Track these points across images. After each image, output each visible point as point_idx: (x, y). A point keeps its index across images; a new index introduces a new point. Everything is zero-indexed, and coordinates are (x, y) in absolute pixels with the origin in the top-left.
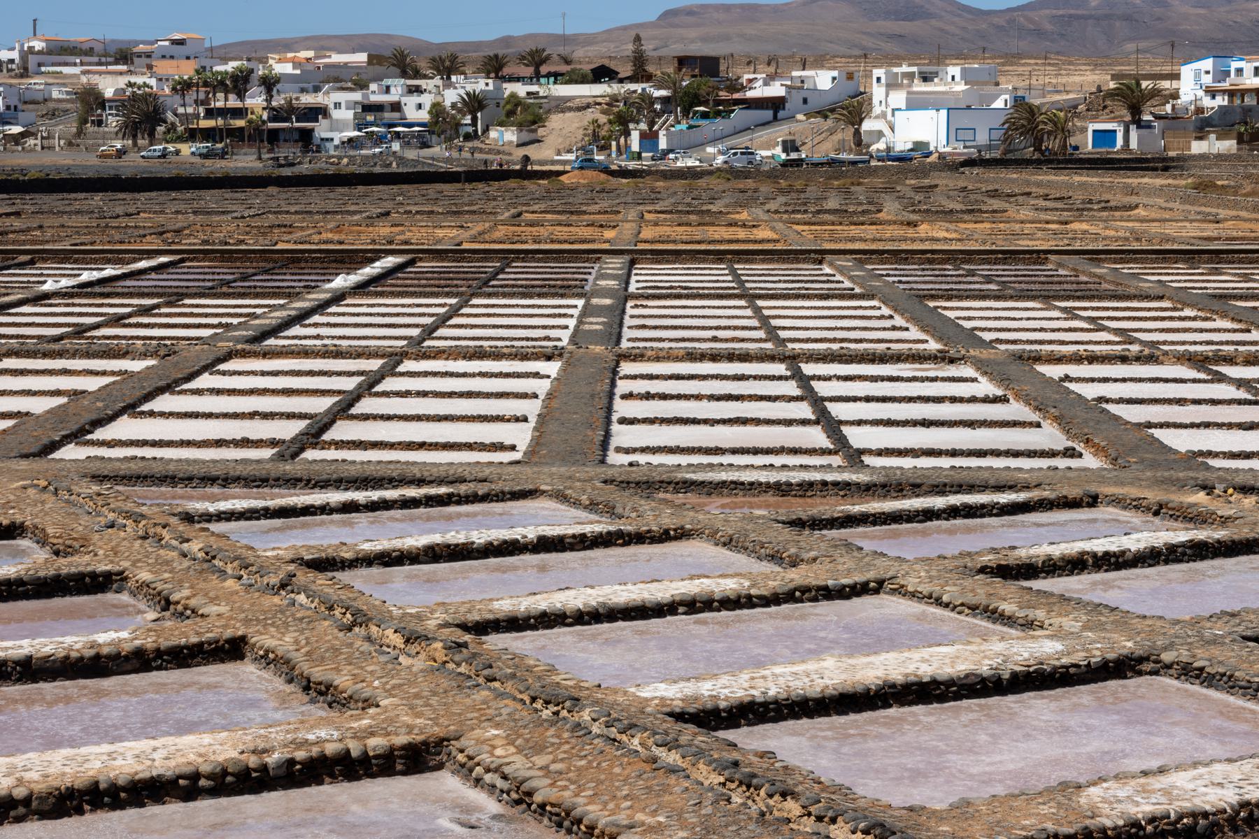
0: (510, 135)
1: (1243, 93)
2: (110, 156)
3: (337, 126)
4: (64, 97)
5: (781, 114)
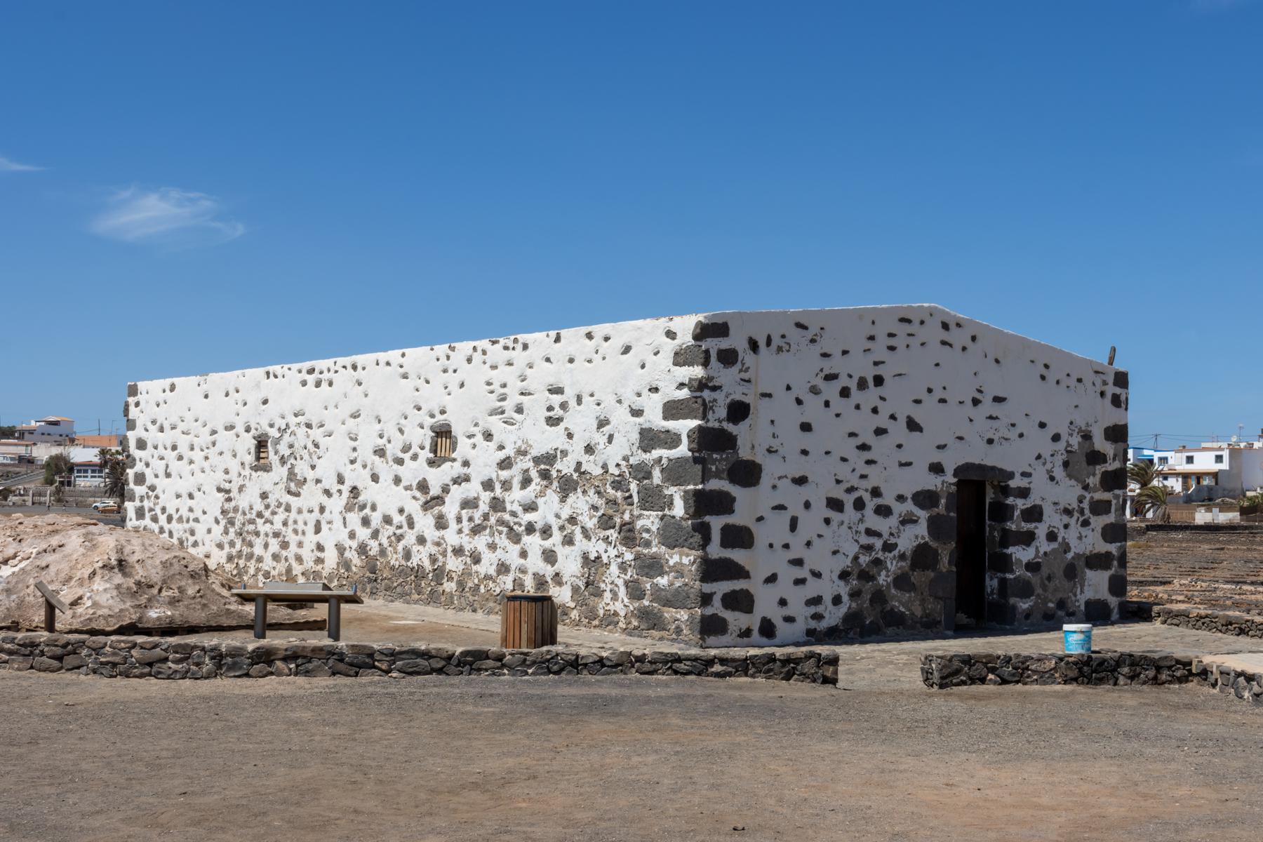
1: (1199, 476)
2: (112, 511)
4: (9, 462)
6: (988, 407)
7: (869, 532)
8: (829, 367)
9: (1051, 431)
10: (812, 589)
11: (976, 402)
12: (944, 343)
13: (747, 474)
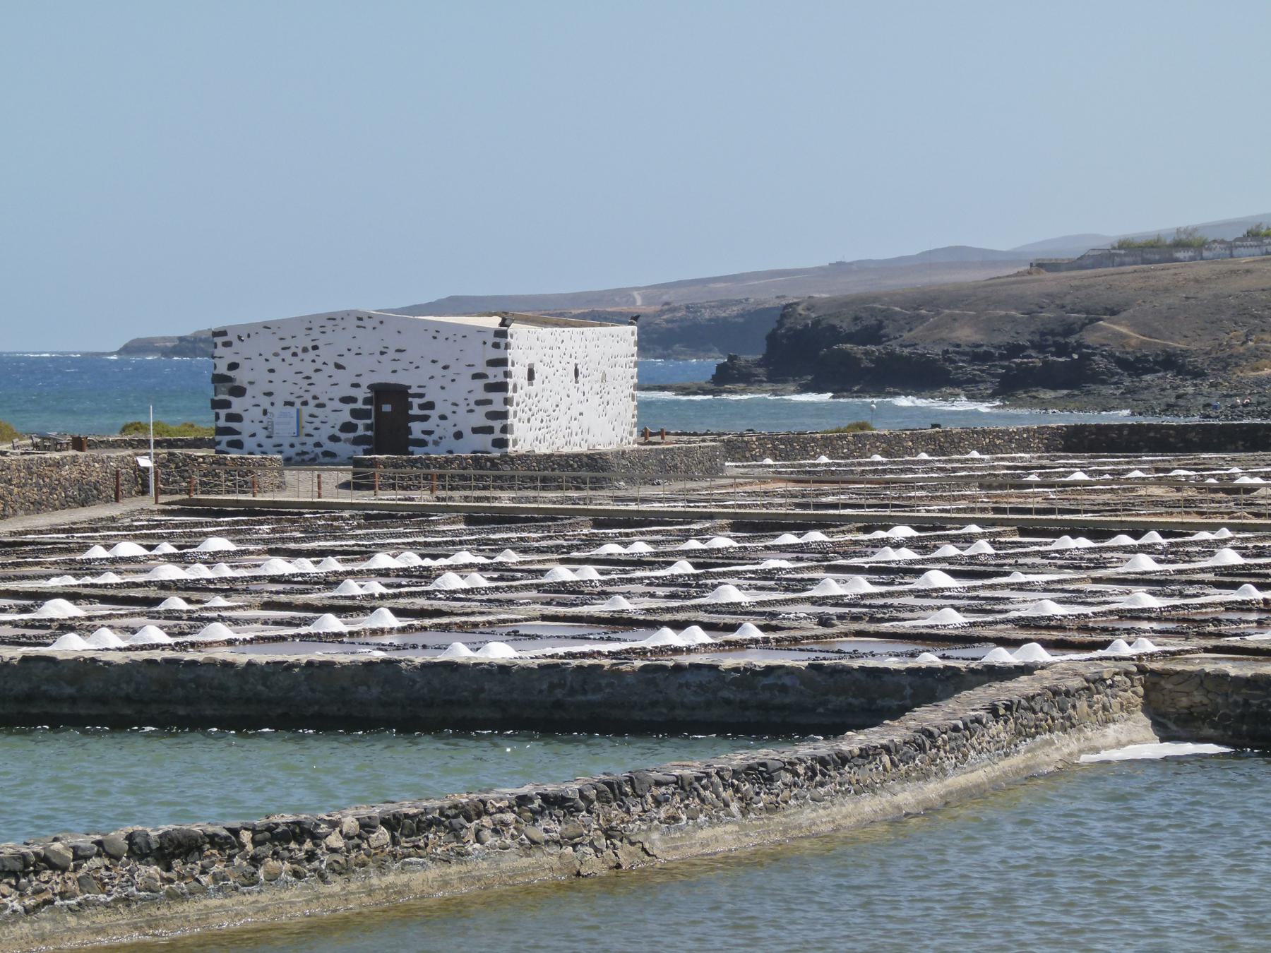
6: (391, 354)
7: (312, 416)
8: (284, 344)
9: (441, 364)
11: (382, 353)
12: (358, 327)
13: (239, 392)
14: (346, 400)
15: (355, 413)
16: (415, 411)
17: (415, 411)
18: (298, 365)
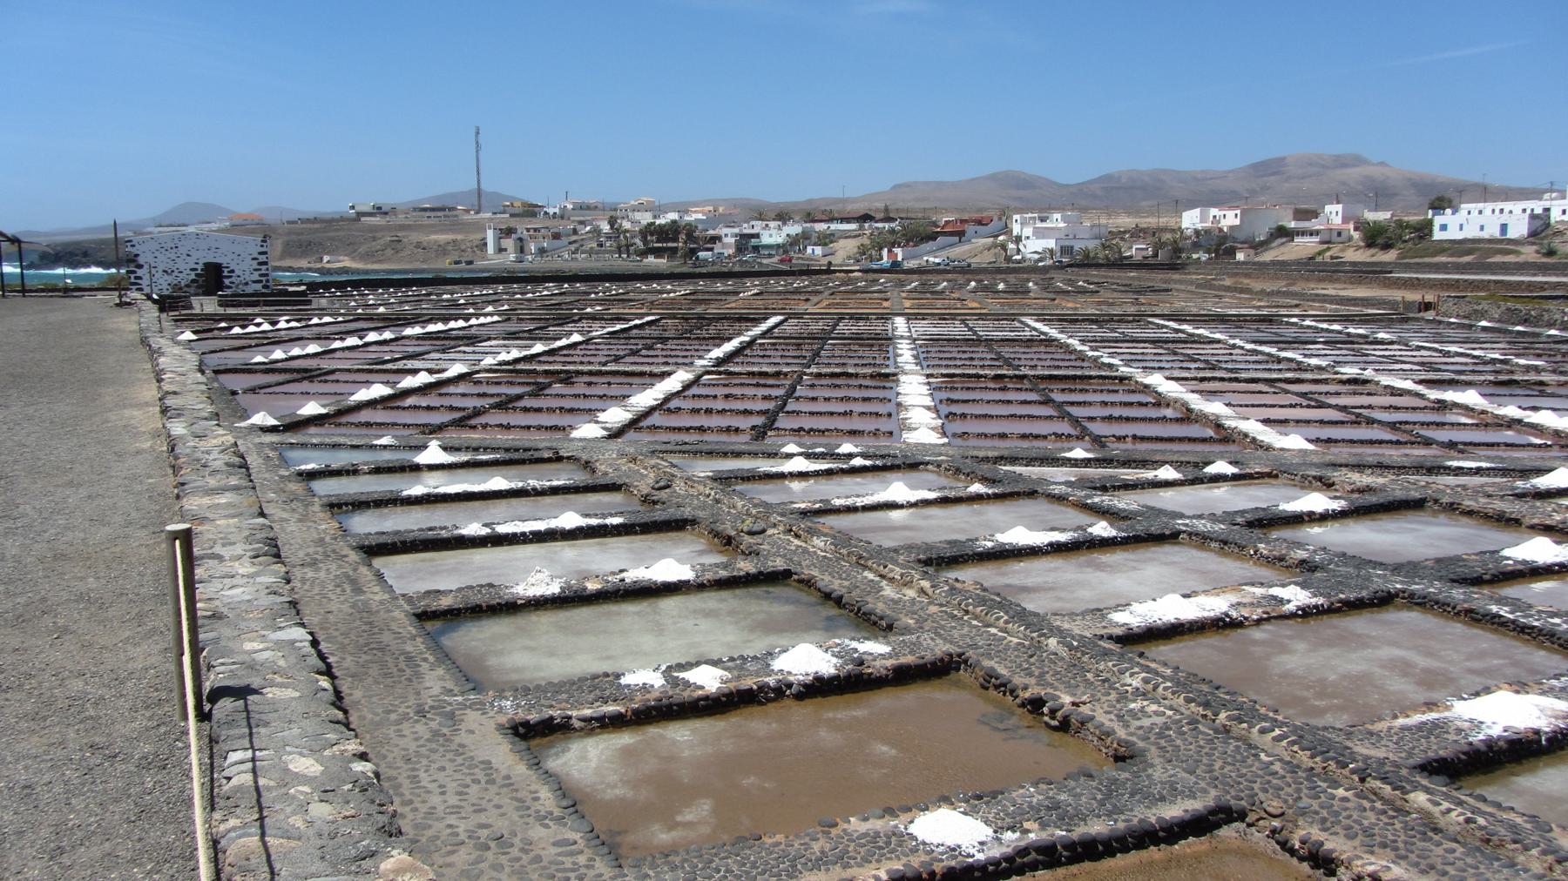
0: (819, 250)
3: (725, 246)
5: (963, 239)
10: (160, 287)
13: (140, 267)
14: (192, 270)
15: (196, 275)
16: (226, 274)
17: (226, 274)
18: (170, 255)
